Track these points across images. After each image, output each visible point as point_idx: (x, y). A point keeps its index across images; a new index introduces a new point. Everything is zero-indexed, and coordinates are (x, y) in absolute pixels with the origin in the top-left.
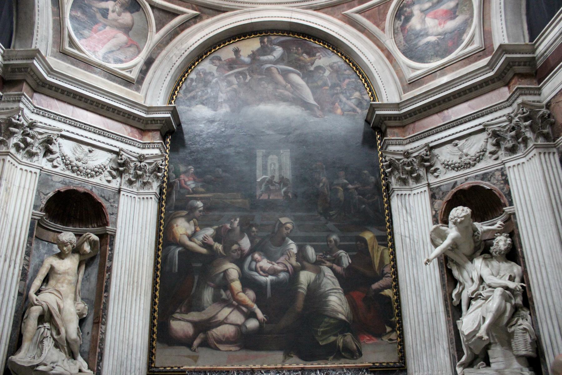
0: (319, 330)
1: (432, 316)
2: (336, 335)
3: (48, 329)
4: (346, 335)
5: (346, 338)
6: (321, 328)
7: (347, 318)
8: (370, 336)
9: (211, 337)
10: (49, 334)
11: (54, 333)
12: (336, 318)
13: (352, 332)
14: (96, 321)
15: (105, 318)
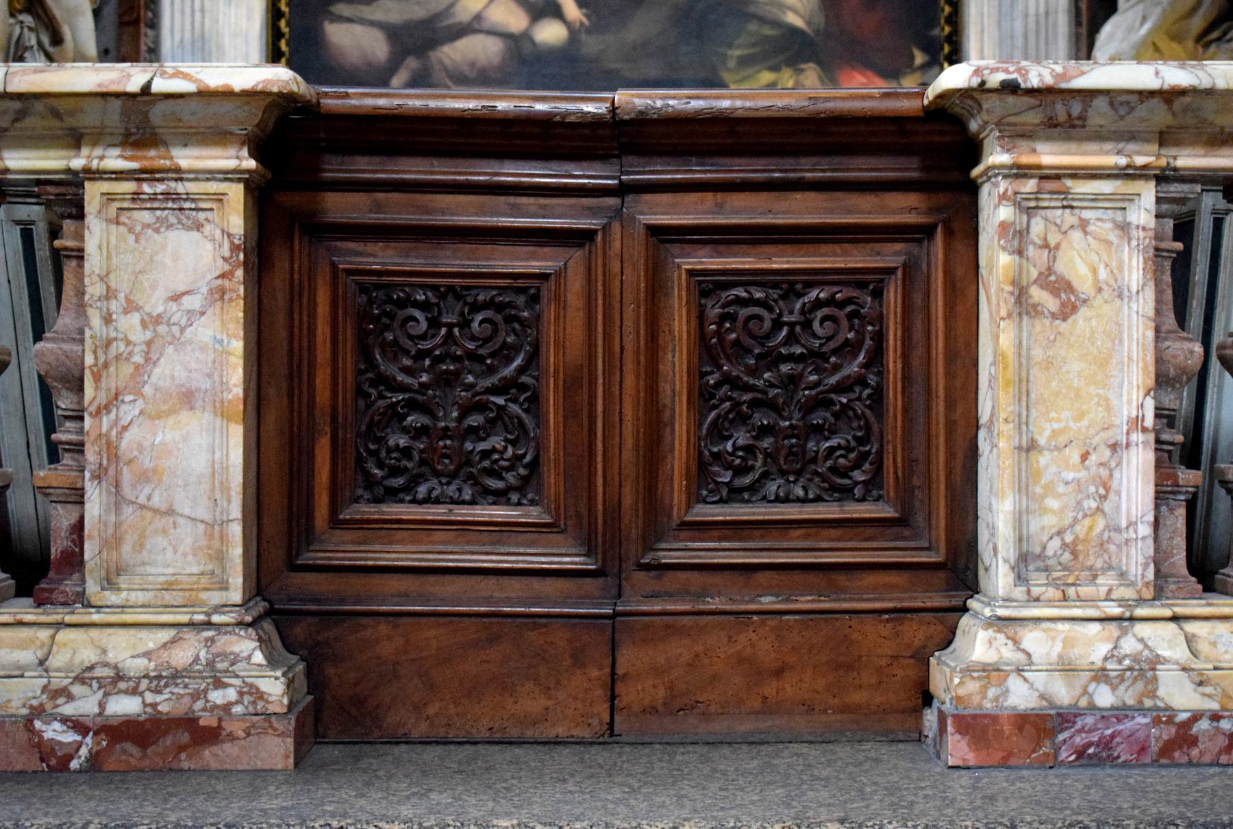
0: (730, 52)
1: (1037, 23)
2: (775, 69)
3: (30, 29)
4: (802, 70)
5: (801, 77)
6: (738, 47)
7: (808, 23)
8: (870, 73)
9: (437, 67)
10: (33, 42)
11: (46, 40)
12: (776, 24)
13: (819, 62)
14: (127, 18)
15: (152, 11)
